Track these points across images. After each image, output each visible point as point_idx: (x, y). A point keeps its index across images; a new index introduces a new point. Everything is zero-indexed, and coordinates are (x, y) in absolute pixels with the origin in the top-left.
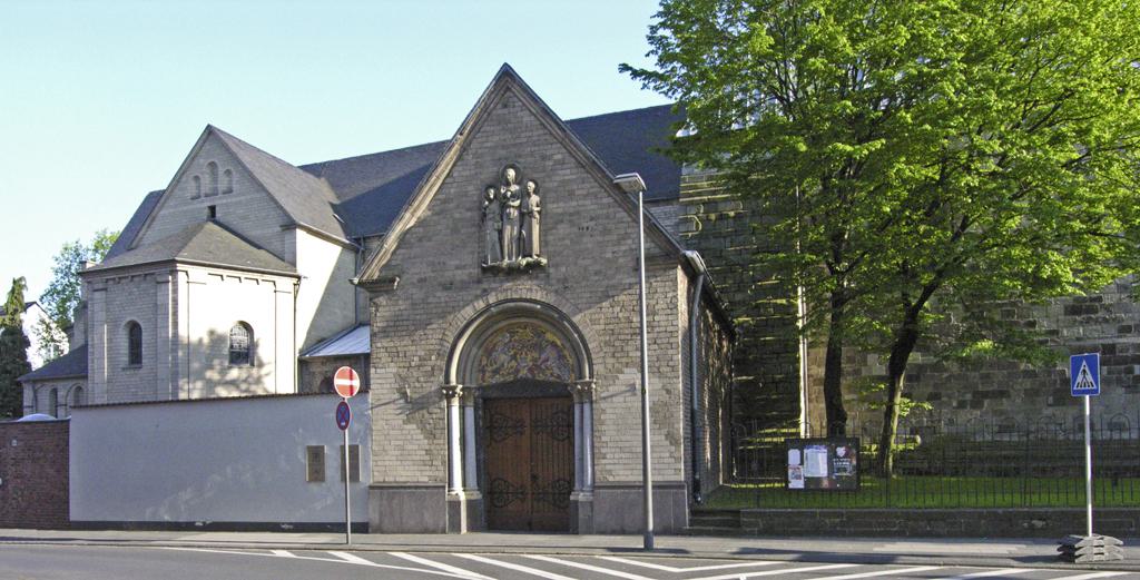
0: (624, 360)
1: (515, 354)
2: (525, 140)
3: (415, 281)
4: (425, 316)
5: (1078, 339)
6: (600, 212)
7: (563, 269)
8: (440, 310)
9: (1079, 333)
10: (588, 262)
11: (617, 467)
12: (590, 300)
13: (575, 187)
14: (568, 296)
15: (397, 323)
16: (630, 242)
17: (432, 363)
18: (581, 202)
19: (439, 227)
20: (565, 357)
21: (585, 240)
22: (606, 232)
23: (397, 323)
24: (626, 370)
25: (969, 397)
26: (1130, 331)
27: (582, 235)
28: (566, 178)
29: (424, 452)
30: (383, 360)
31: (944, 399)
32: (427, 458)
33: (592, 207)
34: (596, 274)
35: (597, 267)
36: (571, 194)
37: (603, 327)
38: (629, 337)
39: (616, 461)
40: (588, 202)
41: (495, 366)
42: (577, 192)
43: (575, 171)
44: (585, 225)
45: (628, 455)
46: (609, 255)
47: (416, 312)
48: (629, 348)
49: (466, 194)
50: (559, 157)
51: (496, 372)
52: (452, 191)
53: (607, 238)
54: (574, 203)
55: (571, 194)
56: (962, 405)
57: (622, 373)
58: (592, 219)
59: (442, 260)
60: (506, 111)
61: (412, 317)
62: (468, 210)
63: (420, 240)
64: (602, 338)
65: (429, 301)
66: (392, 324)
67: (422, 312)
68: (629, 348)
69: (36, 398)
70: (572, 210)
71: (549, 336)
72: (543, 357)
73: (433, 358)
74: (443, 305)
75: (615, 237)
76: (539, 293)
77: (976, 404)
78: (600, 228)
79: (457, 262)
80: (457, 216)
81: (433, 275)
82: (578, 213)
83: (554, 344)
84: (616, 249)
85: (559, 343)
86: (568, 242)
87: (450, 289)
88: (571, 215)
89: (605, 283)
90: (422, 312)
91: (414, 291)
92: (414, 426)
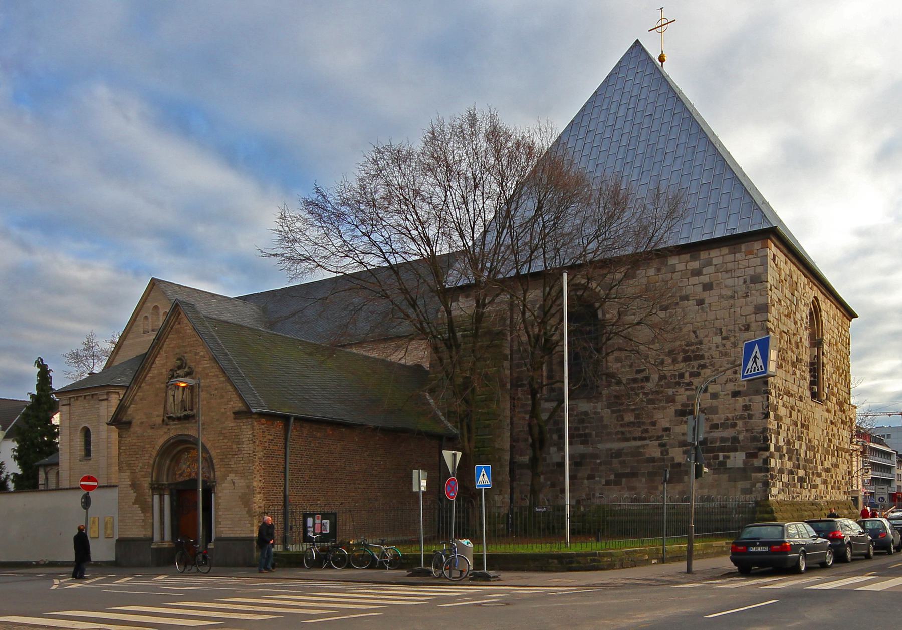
1: (190, 464)
2: (187, 343)
3: (139, 423)
4: (142, 444)
6: (220, 385)
16: (232, 403)
17: (145, 470)
22: (222, 397)
24: (230, 475)
25: (612, 477)
26: (717, 428)
30: (124, 469)
31: (597, 479)
32: (143, 524)
38: (230, 456)
41: (180, 472)
43: (209, 362)
44: (213, 393)
45: (230, 523)
46: (223, 410)
49: (161, 374)
50: (202, 353)
51: (181, 475)
52: (156, 371)
54: (209, 380)
56: (608, 483)
58: (216, 389)
60: (179, 326)
62: (162, 383)
65: (145, 434)
69: (47, 479)
73: (146, 467)
77: (617, 483)
80: (158, 386)
82: (210, 386)
87: (153, 428)
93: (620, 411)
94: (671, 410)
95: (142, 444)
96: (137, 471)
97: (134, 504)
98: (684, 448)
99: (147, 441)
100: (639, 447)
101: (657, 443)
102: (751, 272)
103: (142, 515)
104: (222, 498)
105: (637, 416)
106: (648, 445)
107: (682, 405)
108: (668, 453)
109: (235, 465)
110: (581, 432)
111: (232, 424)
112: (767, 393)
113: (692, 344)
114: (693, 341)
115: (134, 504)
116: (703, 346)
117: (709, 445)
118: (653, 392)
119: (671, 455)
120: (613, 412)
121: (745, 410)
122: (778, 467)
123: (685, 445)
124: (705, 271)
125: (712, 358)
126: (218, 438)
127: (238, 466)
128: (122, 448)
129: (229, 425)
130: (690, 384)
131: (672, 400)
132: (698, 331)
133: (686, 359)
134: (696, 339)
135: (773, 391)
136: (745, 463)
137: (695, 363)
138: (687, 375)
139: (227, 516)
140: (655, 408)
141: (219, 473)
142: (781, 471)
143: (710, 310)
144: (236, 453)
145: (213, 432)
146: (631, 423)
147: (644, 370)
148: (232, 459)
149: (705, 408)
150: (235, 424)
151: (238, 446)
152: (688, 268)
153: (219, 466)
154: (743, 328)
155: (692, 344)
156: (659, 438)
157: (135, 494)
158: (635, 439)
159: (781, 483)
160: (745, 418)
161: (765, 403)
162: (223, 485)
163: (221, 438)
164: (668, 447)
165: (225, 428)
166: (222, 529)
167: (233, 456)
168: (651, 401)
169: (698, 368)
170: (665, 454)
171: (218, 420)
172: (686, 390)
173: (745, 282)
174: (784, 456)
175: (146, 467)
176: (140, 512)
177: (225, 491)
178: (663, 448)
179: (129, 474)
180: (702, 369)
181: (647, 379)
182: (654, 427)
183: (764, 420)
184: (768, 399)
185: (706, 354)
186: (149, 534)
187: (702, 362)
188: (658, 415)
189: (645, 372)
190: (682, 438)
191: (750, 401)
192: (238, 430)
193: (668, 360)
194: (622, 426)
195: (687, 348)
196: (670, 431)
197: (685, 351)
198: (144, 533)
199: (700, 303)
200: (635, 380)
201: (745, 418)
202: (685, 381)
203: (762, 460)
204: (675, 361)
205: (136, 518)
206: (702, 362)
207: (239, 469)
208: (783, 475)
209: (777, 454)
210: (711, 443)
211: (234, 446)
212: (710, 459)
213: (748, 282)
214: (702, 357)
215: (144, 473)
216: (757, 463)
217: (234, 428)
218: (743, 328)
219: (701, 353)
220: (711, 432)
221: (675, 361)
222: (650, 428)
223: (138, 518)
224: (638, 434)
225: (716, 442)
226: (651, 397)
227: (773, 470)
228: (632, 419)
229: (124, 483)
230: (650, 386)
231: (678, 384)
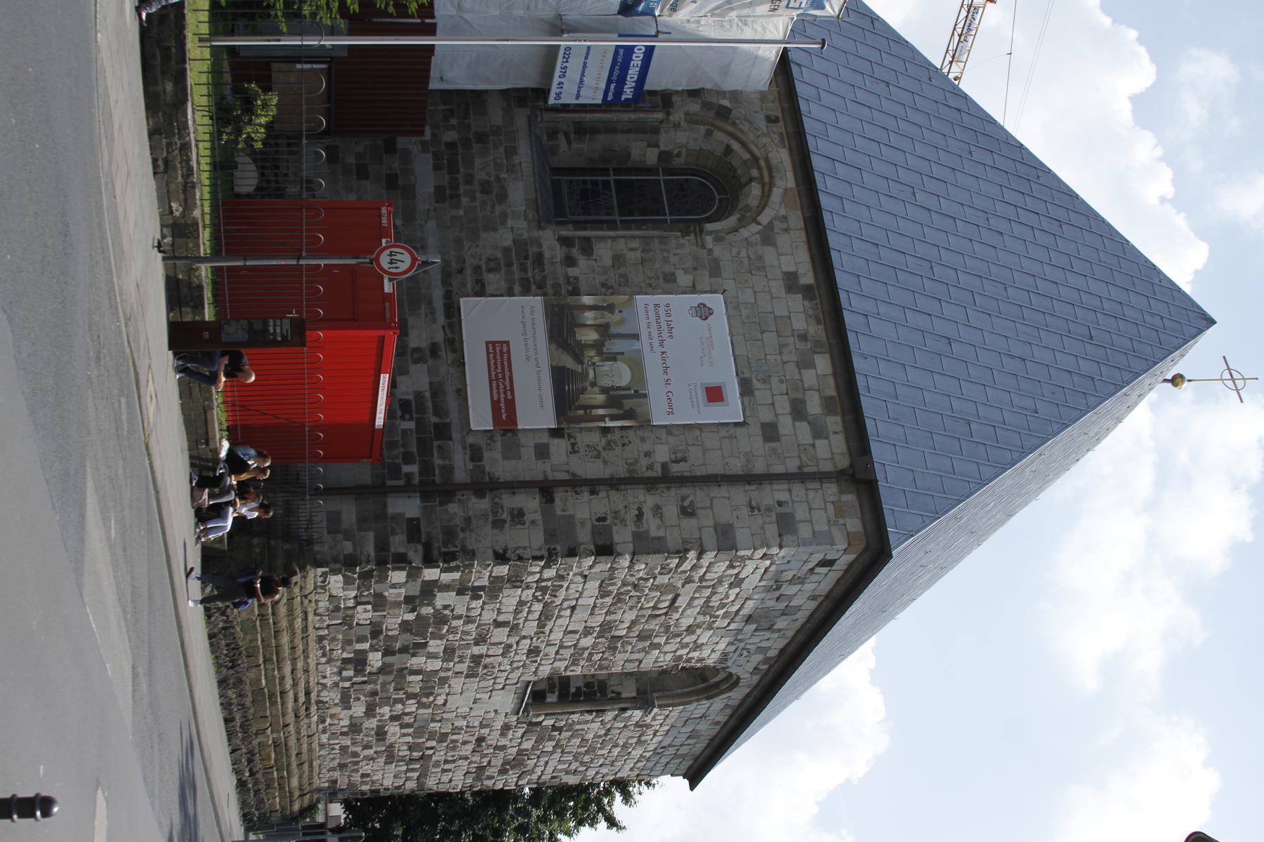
98: (428, 395)
100: (430, 302)
101: (439, 337)
106: (434, 321)
108: (417, 361)
112: (550, 555)
117: (436, 443)
119: (413, 368)
120: (506, 250)
121: (512, 514)
122: (390, 594)
123: (435, 394)
125: (624, 445)
135: (550, 573)
136: (397, 517)
142: (379, 602)
143: (724, 437)
159: (351, 603)
160: (495, 514)
161: (527, 554)
164: (430, 361)
170: (416, 356)
174: (413, 611)
178: (427, 352)
183: (490, 552)
184: (536, 558)
191: (533, 522)
194: (477, 269)
201: (495, 514)
208: (369, 607)
209: (415, 589)
210: (440, 447)
212: (403, 446)
216: (398, 543)
218: (686, 503)
220: (464, 447)
227: (383, 578)
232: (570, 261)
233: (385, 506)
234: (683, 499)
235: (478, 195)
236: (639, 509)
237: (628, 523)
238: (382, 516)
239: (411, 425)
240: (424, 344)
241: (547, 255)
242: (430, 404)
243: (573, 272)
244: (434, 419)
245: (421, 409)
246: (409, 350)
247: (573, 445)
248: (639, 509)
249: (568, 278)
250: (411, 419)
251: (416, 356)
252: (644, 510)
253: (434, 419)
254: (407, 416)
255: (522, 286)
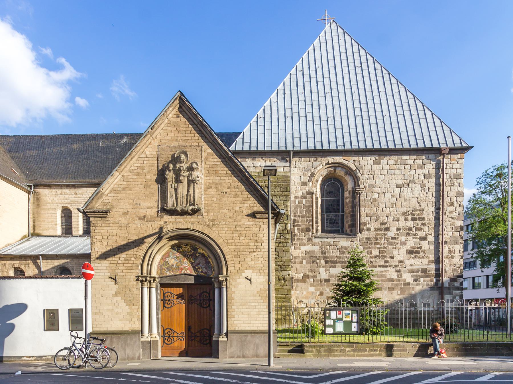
0: (246, 266)
4: (127, 235)
5: (411, 265)
6: (233, 184)
7: (212, 214)
8: (138, 232)
9: (412, 262)
10: (225, 211)
11: (240, 322)
12: (227, 232)
13: (219, 169)
14: (215, 229)
15: (109, 238)
17: (132, 262)
18: (223, 178)
19: (136, 183)
20: (209, 262)
21: (225, 199)
23: (109, 238)
24: (246, 271)
27: (223, 196)
28: (214, 163)
29: (126, 314)
32: (129, 316)
33: (229, 181)
34: (230, 218)
35: (231, 215)
36: (217, 172)
37: (233, 247)
38: (248, 253)
39: (240, 319)
40: (226, 178)
42: (220, 172)
44: (225, 191)
45: (246, 316)
46: (238, 209)
47: (121, 231)
48: (248, 259)
52: (145, 162)
53: (237, 199)
54: (218, 178)
55: (217, 172)
57: (244, 272)
58: (229, 188)
59: (138, 203)
61: (120, 234)
63: (124, 189)
64: (233, 253)
66: (106, 237)
67: (126, 231)
68: (248, 259)
70: (218, 182)
71: (200, 251)
72: (197, 261)
73: (133, 259)
74: (139, 229)
75: (241, 199)
76: (198, 226)
78: (233, 193)
79: (149, 205)
80: (148, 177)
81: (132, 210)
82: (220, 184)
83: (203, 255)
84: (241, 205)
85: (206, 255)
86: (214, 199)
87: (143, 220)
88: (217, 184)
89: (236, 223)
90: (126, 231)
91: (120, 219)
92: (120, 298)
93: (370, 248)
94: (403, 250)
95: (127, 235)
96: (119, 262)
97: (116, 295)
98: (412, 274)
99: (133, 232)
100: (382, 272)
101: (394, 270)
102: (454, 171)
103: (128, 307)
104: (236, 292)
105: (381, 252)
106: (388, 271)
107: (411, 247)
108: (401, 276)
109: (253, 262)
110: (342, 260)
111: (250, 223)
113: (417, 210)
114: (418, 208)
115: (116, 295)
116: (424, 212)
117: (427, 272)
118: (392, 238)
121: (450, 253)
123: (412, 272)
124: (426, 167)
126: (232, 235)
127: (256, 262)
128: (96, 237)
129: (246, 224)
130: (415, 235)
131: (404, 244)
132: (421, 203)
133: (413, 219)
134: (420, 208)
136: (449, 284)
137: (418, 222)
138: (414, 229)
139: (242, 310)
140: (393, 248)
141: (233, 268)
143: (429, 191)
144: (255, 250)
145: (226, 229)
146: (377, 256)
147: (386, 223)
148: (249, 256)
149: (425, 250)
150: (253, 223)
151: (257, 244)
152: (415, 163)
153: (233, 262)
154: (449, 204)
155: (417, 210)
156: (396, 267)
157: (117, 286)
158: (380, 266)
160: (449, 258)
162: (238, 281)
163: (236, 235)
164: (401, 273)
165: (241, 226)
166: (235, 322)
167: (251, 254)
168: (390, 244)
169: (421, 225)
170: (400, 276)
171: (230, 218)
172: (414, 238)
173: (450, 177)
175: (133, 259)
176: (125, 304)
177: (239, 286)
178: (399, 273)
179: (108, 265)
180: (423, 226)
181: (387, 229)
182: (392, 260)
185: (426, 217)
186: (137, 327)
187: (423, 222)
188: (395, 253)
189: (386, 225)
190: (410, 268)
191: (452, 248)
192: (258, 229)
193: (402, 218)
195: (414, 212)
196: (403, 263)
197: (413, 215)
198: (130, 326)
199: (422, 186)
200: (380, 229)
201: (449, 258)
202: (413, 233)
203: (459, 283)
204: (406, 219)
205: (116, 310)
206: (423, 222)
207: (258, 265)
210: (429, 271)
211: (252, 244)
212: (428, 281)
213: (452, 177)
214: (423, 219)
215: (130, 265)
216: (457, 284)
217: (252, 227)
218: (449, 204)
219: (423, 216)
221: (406, 219)
222: (390, 260)
223: (121, 311)
224: (382, 263)
225: (432, 271)
226: (391, 240)
228: (378, 254)
229: (101, 274)
230: (390, 234)
231: (408, 234)
232: (369, 230)
233: (446, 287)
234: (447, 205)
235: (344, 255)
236: (450, 218)
237: (454, 221)
238: (449, 288)
239: (422, 279)
240: (396, 274)
241: (366, 236)
242: (415, 274)
243: (372, 229)
244: (420, 272)
245: (417, 276)
246: (398, 278)
247: (429, 234)
248: (450, 218)
249: (374, 231)
250: (420, 279)
251: (400, 276)
252: (450, 216)
253: (420, 272)
254: (419, 280)
255: (377, 244)
